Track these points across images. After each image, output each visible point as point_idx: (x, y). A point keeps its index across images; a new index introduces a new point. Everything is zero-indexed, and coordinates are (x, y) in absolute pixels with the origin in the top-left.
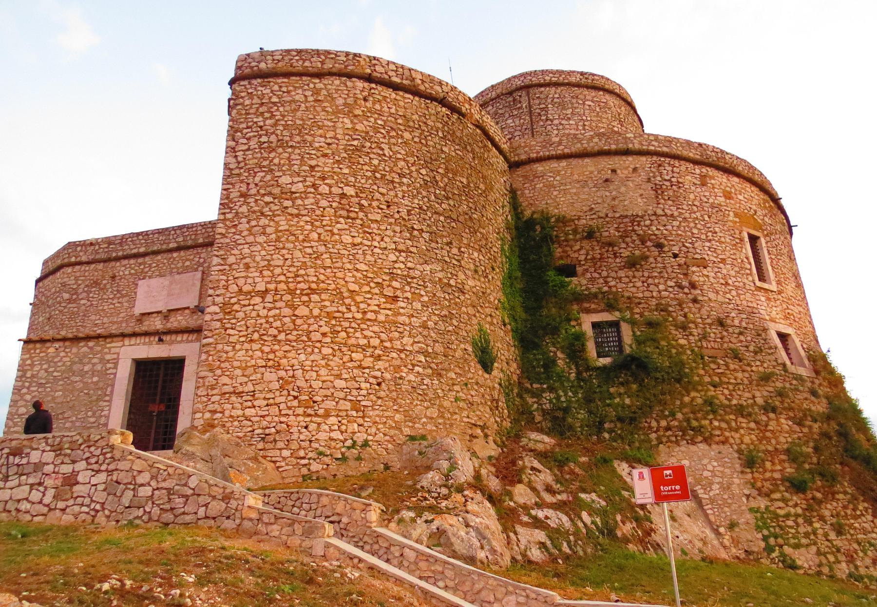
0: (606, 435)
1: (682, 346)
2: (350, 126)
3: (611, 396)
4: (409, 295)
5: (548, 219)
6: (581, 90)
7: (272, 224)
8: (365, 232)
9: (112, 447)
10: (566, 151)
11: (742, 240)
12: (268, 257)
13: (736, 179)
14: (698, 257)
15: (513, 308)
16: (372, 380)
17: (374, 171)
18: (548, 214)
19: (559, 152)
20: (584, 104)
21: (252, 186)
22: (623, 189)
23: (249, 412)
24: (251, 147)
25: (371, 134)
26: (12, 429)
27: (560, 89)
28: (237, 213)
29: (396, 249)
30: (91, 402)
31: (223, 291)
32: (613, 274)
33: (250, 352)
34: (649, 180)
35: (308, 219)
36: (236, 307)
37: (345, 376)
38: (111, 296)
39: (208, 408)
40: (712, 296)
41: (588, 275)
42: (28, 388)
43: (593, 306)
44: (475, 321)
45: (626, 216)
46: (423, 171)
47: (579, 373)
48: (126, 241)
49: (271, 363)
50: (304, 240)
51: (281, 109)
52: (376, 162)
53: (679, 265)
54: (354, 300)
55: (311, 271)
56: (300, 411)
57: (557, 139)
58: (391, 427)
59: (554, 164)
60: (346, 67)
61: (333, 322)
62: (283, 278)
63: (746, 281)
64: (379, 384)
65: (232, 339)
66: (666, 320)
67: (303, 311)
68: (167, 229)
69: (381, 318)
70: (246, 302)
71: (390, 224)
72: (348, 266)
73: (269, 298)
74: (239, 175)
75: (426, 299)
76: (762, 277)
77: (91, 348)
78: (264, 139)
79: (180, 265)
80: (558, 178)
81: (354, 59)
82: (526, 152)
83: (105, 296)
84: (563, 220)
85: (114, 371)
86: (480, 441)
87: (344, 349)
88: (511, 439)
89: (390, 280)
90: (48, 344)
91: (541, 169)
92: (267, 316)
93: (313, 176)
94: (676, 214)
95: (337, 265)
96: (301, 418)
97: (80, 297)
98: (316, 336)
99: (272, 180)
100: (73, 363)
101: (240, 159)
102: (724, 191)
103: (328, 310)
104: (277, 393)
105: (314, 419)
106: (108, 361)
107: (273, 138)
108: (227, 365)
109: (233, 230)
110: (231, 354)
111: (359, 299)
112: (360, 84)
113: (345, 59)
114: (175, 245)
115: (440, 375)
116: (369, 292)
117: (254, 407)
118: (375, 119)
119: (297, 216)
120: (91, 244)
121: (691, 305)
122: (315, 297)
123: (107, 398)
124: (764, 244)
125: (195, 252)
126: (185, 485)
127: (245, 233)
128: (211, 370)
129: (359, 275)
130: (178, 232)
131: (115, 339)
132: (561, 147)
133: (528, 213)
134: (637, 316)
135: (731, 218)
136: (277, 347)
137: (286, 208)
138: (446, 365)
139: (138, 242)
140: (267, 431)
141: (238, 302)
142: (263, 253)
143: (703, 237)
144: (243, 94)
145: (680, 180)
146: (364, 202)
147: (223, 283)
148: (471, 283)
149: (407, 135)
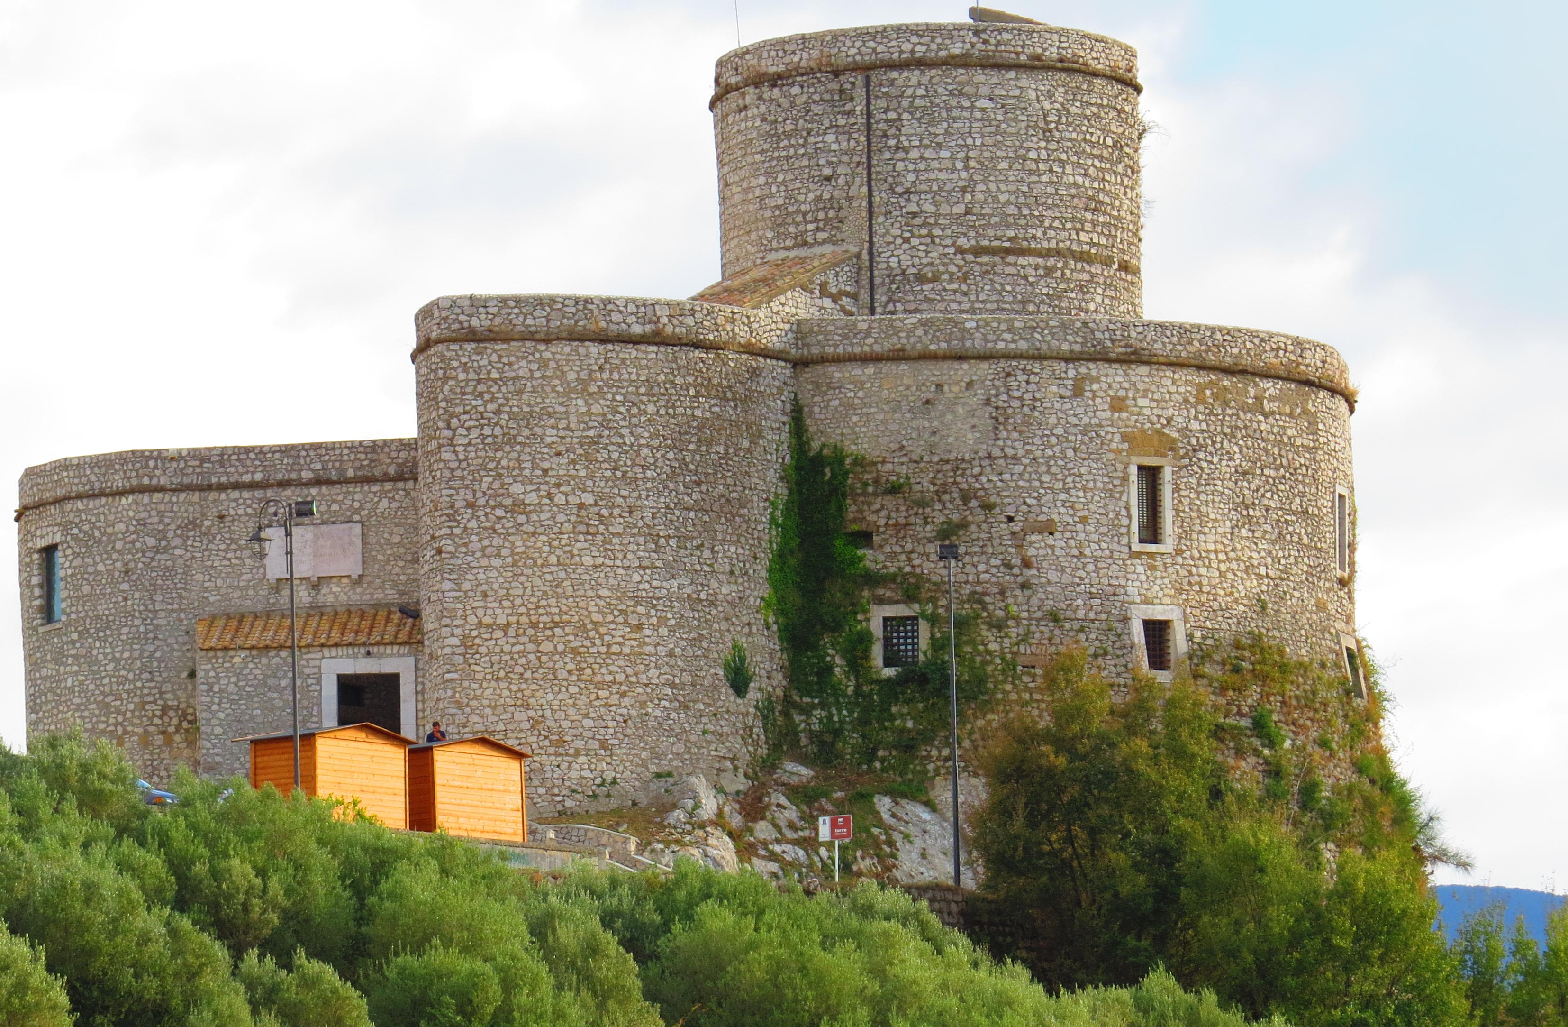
0: (878, 765)
1: (989, 652)
2: (584, 409)
3: (892, 718)
4: (654, 620)
5: (841, 461)
8: (606, 550)
10: (877, 348)
11: (1125, 479)
12: (506, 585)
14: (1042, 518)
15: (781, 600)
17: (615, 469)
18: (842, 450)
19: (867, 349)
22: (949, 417)
28: (466, 528)
29: (640, 567)
31: (462, 622)
32: (920, 549)
34: (988, 402)
35: (545, 538)
36: (477, 641)
37: (592, 715)
38: (223, 547)
40: (1053, 576)
41: (887, 549)
43: (888, 594)
44: (728, 637)
45: (947, 462)
46: (671, 455)
47: (858, 687)
48: (229, 460)
49: (519, 702)
50: (542, 565)
51: (504, 389)
52: (615, 456)
53: (1013, 533)
54: (597, 632)
55: (553, 601)
56: (552, 750)
57: (864, 326)
58: (637, 765)
59: (857, 371)
60: (577, 322)
62: (523, 610)
63: (1115, 546)
66: (978, 616)
67: (547, 647)
68: (293, 447)
69: (627, 650)
70: (488, 636)
72: (591, 593)
73: (511, 632)
74: (462, 478)
75: (673, 622)
78: (487, 431)
81: (585, 308)
82: (819, 342)
83: (211, 546)
84: (860, 462)
86: (729, 775)
87: (591, 687)
88: (764, 770)
89: (635, 606)
91: (837, 375)
93: (547, 483)
94: (1021, 453)
96: (552, 758)
99: (502, 487)
101: (461, 457)
103: (573, 645)
107: (498, 431)
108: (474, 703)
110: (478, 692)
111: (603, 630)
112: (594, 349)
113: (573, 310)
115: (687, 708)
116: (613, 622)
118: (614, 395)
119: (534, 534)
120: (172, 459)
121: (1018, 592)
122: (558, 631)
125: (344, 490)
128: (459, 708)
129: (602, 603)
130: (312, 453)
132: (870, 341)
133: (815, 445)
134: (940, 611)
136: (524, 686)
137: (521, 525)
139: (249, 463)
142: (501, 580)
144: (455, 364)
145: (1037, 395)
146: (605, 512)
147: (460, 613)
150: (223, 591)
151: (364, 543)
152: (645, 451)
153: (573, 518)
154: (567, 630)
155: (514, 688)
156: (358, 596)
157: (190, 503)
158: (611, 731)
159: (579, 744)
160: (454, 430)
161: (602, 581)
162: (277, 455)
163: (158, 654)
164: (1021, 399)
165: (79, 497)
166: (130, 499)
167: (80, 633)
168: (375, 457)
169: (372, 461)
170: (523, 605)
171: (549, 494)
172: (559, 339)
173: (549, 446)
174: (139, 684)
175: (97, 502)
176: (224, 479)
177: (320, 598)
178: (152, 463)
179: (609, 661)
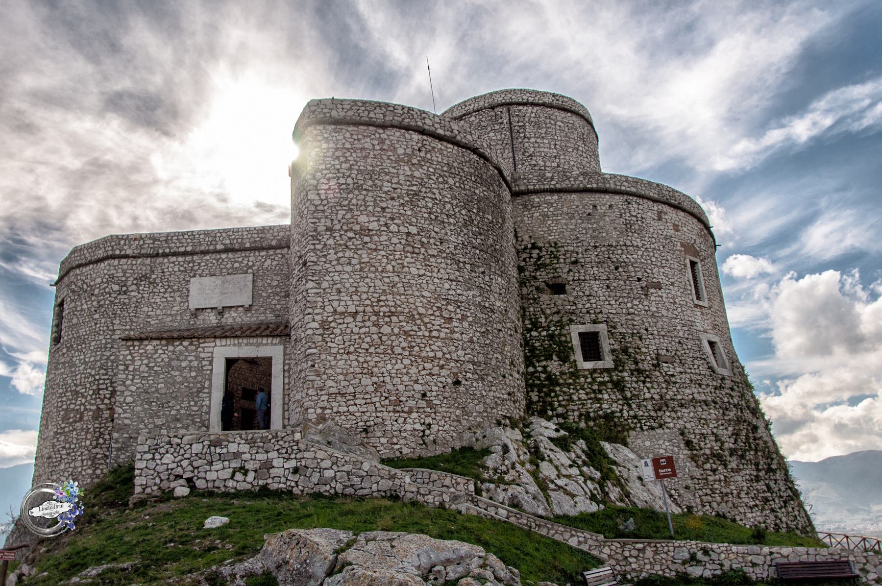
2: (409, 173)
6: (553, 110)
7: (356, 256)
8: (426, 265)
9: (297, 443)
10: (558, 186)
11: (685, 266)
12: (356, 285)
13: (682, 214)
14: (654, 280)
16: (439, 384)
17: (430, 213)
19: (552, 186)
20: (555, 124)
21: (335, 222)
23: (352, 409)
24: (332, 187)
25: (426, 180)
26: (122, 416)
27: (536, 108)
28: (325, 245)
30: (191, 394)
31: (321, 311)
33: (349, 362)
35: (384, 253)
36: (333, 325)
39: (319, 405)
40: (664, 312)
42: (132, 380)
46: (463, 212)
48: (171, 239)
49: (365, 371)
50: (382, 272)
51: (354, 155)
53: (642, 288)
54: (422, 321)
55: (390, 297)
56: (391, 408)
57: (550, 175)
61: (410, 339)
62: (368, 302)
64: (444, 387)
65: (334, 351)
69: (443, 335)
70: (339, 321)
71: (444, 258)
72: (417, 293)
73: (359, 318)
74: (323, 211)
75: (471, 319)
76: (698, 298)
77: (186, 347)
78: (342, 181)
79: (228, 266)
80: (551, 209)
81: (408, 112)
85: (210, 367)
87: (419, 360)
89: (447, 305)
90: (146, 342)
92: (358, 333)
93: (385, 217)
94: (640, 245)
95: (408, 292)
97: (130, 289)
98: (398, 350)
99: (352, 217)
100: (171, 359)
102: (674, 225)
103: (405, 329)
104: (373, 395)
105: (402, 414)
106: (203, 359)
108: (330, 371)
109: (324, 260)
110: (333, 363)
111: (426, 320)
112: (416, 136)
114: (223, 247)
117: (356, 405)
119: (375, 250)
120: (136, 239)
122: (394, 319)
123: (206, 391)
124: (700, 269)
125: (243, 255)
126: (360, 469)
127: (334, 263)
128: (318, 375)
129: (425, 301)
130: (224, 235)
131: (207, 340)
135: (678, 248)
136: (369, 358)
137: (366, 243)
138: (486, 371)
139: (184, 241)
140: (368, 424)
141: (334, 320)
142: (351, 281)
143: (659, 264)
147: (320, 304)
148: (498, 304)
149: (451, 181)
150: (160, 317)
151: (254, 286)
152: (448, 206)
153: (403, 242)
154: (401, 318)
155: (361, 360)
156: (248, 319)
157: (144, 265)
158: (434, 394)
159: (412, 403)
160: (318, 181)
161: (425, 286)
162: (202, 236)
163: (112, 358)
164: (636, 216)
165: (79, 266)
166: (106, 262)
167: (68, 348)
168: (264, 236)
169: (261, 238)
170: (368, 299)
171: (386, 224)
172: (393, 126)
173: (386, 193)
174: (97, 377)
175: (88, 268)
176: (167, 251)
177: (224, 320)
178: (122, 242)
179: (430, 342)
